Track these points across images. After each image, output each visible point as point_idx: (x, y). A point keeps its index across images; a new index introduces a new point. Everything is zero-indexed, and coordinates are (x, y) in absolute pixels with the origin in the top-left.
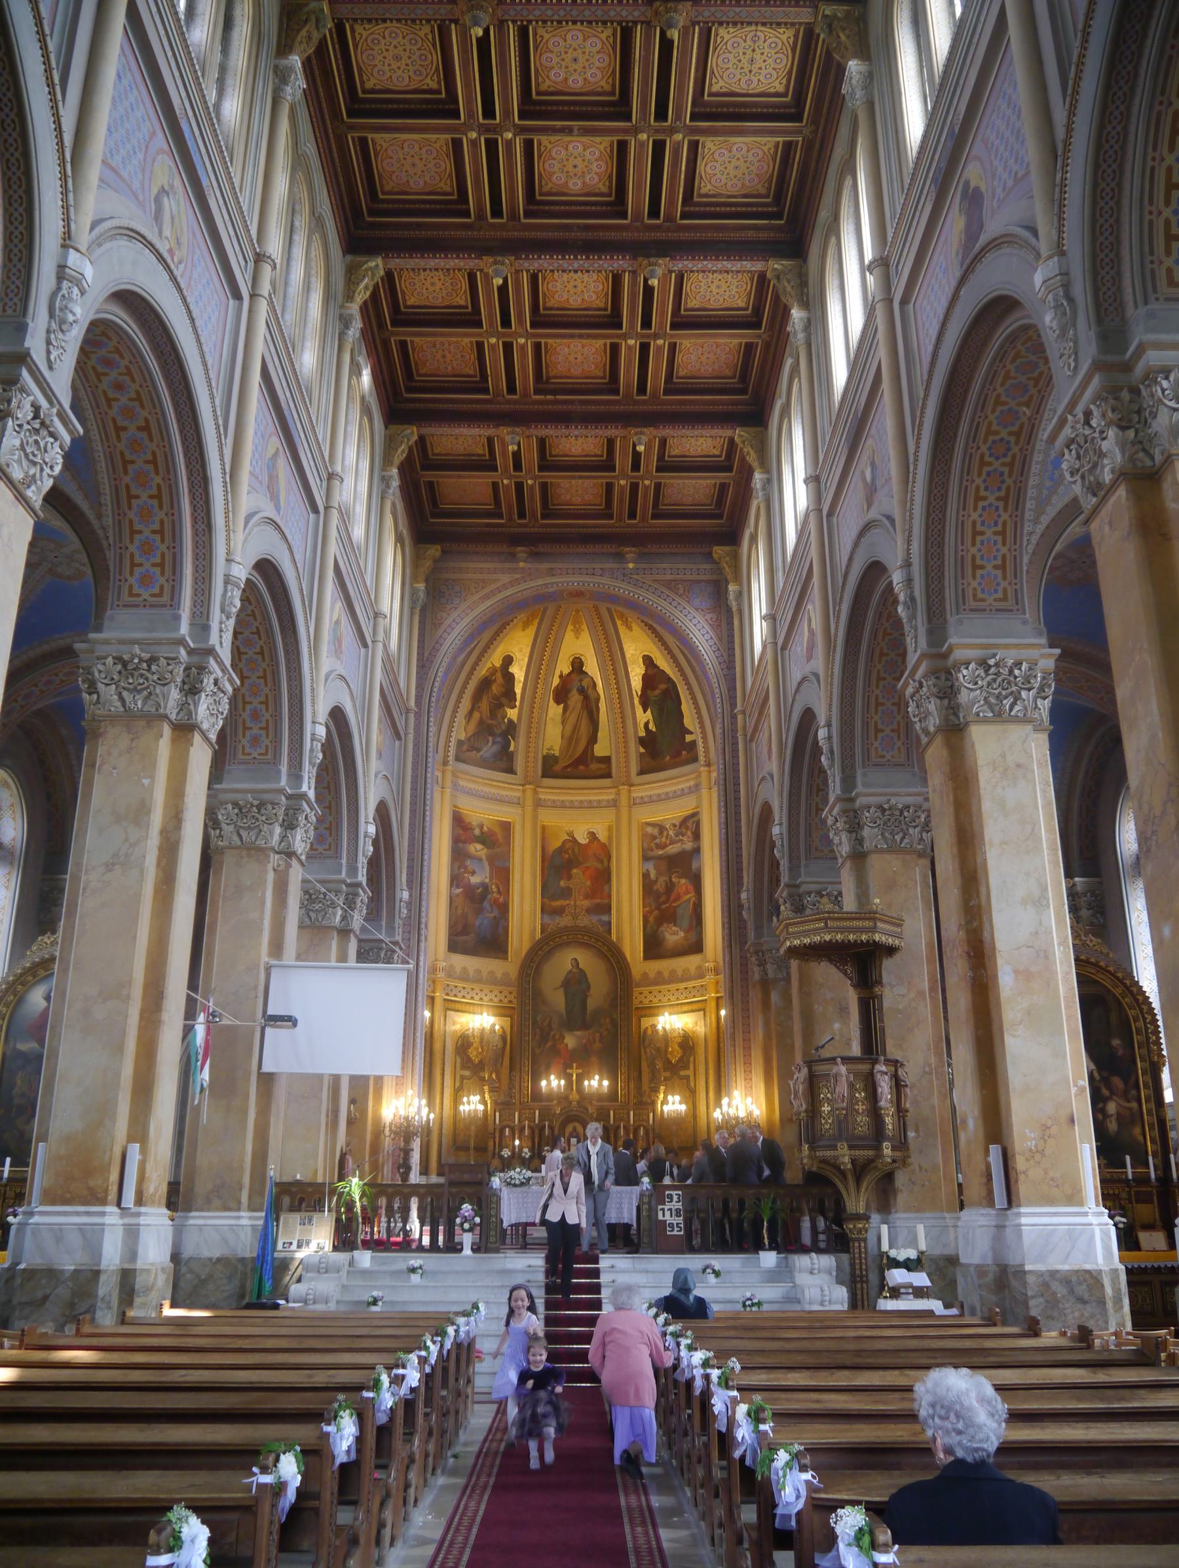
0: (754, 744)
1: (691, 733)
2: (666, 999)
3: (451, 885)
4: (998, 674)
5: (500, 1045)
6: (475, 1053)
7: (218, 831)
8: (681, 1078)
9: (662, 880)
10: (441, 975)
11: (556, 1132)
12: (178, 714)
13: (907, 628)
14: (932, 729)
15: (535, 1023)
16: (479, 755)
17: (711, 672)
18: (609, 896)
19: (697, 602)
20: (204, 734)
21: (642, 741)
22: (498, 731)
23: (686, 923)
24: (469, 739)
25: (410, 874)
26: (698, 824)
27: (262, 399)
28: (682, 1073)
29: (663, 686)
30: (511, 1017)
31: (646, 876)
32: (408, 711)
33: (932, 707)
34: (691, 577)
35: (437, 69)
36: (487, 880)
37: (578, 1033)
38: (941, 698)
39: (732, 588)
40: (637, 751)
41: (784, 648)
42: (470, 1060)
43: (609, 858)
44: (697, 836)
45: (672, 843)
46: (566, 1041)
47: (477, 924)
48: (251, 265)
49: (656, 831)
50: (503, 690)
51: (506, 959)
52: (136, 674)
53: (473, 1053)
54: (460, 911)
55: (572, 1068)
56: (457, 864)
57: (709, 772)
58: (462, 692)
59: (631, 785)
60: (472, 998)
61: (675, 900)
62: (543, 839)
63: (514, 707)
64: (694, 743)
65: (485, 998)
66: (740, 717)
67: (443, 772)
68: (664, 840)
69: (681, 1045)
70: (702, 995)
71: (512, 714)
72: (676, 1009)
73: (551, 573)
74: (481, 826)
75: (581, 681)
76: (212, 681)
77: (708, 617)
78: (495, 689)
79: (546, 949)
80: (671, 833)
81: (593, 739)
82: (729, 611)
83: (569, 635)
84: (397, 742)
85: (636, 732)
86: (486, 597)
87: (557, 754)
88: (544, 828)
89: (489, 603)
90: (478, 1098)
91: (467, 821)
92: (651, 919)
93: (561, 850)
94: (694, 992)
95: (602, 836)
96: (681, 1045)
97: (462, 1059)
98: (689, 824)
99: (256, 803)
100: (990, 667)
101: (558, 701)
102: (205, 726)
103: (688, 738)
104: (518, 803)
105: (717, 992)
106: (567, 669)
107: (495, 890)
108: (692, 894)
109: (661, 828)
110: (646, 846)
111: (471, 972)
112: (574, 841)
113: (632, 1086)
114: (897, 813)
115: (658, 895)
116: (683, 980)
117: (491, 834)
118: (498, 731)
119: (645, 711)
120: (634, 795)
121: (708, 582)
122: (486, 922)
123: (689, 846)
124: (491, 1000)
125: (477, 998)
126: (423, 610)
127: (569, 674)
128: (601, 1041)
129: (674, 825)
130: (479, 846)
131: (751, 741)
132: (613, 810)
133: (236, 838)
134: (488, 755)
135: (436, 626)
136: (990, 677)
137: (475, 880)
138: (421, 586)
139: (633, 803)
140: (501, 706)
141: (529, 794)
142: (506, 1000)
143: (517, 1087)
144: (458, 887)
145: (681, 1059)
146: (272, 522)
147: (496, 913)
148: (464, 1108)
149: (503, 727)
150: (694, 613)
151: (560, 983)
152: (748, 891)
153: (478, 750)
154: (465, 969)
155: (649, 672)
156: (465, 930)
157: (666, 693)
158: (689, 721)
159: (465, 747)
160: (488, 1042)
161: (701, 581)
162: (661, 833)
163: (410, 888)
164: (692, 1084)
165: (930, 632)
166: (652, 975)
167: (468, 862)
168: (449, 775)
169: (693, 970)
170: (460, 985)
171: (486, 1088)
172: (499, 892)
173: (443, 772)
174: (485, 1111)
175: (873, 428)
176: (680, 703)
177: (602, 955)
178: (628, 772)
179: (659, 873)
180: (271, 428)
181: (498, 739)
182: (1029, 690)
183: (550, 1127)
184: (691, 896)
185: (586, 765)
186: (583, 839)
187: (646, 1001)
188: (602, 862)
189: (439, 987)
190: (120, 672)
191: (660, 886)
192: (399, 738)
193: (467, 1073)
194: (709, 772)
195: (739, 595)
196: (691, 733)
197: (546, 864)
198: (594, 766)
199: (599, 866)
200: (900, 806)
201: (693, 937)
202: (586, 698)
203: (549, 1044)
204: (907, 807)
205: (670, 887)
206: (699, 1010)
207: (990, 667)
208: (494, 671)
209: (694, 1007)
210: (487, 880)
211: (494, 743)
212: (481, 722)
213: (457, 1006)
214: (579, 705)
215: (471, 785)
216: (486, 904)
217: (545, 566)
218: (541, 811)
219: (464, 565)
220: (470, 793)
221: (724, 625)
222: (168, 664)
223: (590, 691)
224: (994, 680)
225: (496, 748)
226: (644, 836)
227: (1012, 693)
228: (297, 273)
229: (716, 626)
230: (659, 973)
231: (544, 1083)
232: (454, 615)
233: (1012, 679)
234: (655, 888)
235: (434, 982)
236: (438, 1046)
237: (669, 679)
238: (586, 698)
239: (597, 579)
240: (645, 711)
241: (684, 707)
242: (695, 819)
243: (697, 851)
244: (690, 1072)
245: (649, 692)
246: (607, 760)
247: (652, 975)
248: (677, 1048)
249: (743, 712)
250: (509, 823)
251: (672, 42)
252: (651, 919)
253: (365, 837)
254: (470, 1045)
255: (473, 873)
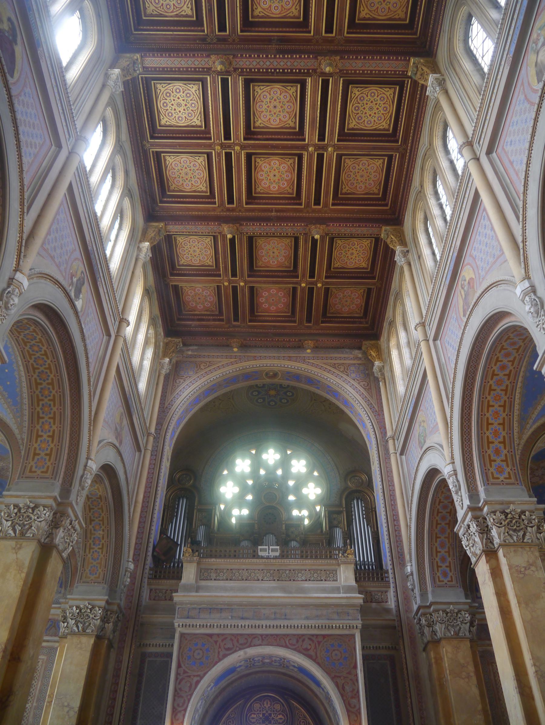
4: (513, 518)
7: (66, 624)
12: (45, 540)
13: (455, 497)
14: (478, 552)
20: (60, 553)
27: (115, 384)
33: (477, 539)
35: (212, 257)
38: (482, 533)
48: (117, 323)
52: (25, 515)
76: (68, 521)
99: (90, 607)
100: (508, 514)
102: (61, 547)
114: (455, 615)
133: (75, 629)
136: (508, 520)
146: (115, 446)
165: (471, 498)
175: (424, 405)
180: (120, 404)
182: (532, 527)
190: (16, 514)
200: (456, 611)
204: (523, 512)
207: (508, 514)
222: (44, 510)
224: (511, 522)
227: (522, 529)
228: (141, 337)
233: (521, 520)
251: (317, 240)
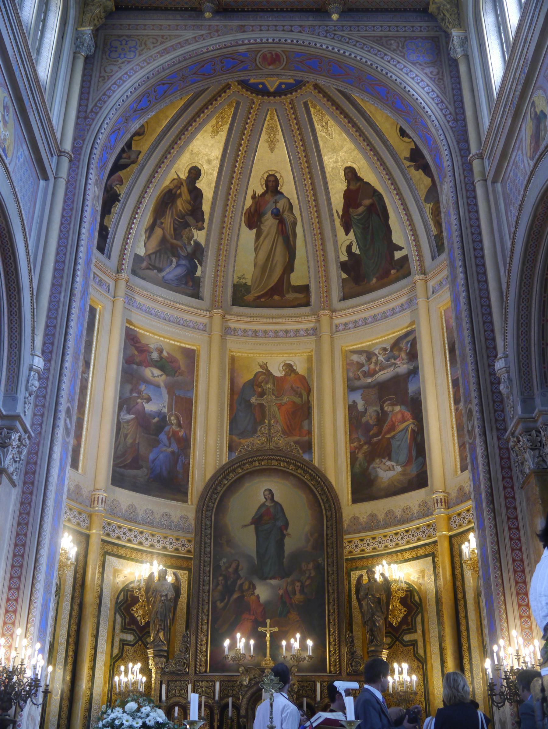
0: (499, 186)
1: (401, 248)
2: (382, 547)
3: (120, 408)
5: (171, 595)
6: (141, 612)
8: (406, 644)
9: (372, 411)
10: (99, 507)
11: (243, 712)
15: (217, 567)
16: (161, 275)
17: (436, 133)
18: (310, 433)
19: (413, 57)
21: (344, 266)
22: (183, 253)
23: (403, 457)
24: (149, 256)
25: (49, 335)
26: (414, 343)
28: (407, 638)
29: (367, 202)
30: (189, 570)
31: (352, 408)
32: (61, 153)
34: (406, 34)
36: (165, 410)
37: (273, 582)
39: (455, 33)
40: (339, 277)
41: (494, 182)
42: (134, 620)
43: (309, 391)
44: (413, 356)
45: (382, 368)
46: (257, 592)
47: (151, 456)
49: (362, 359)
50: (190, 208)
51: (186, 501)
53: (138, 612)
54: (129, 441)
55: (265, 625)
56: (128, 387)
57: (426, 281)
58: (142, 197)
59: (334, 311)
60: (140, 543)
61: (388, 432)
62: (232, 371)
63: (202, 228)
64: (405, 258)
65: (158, 546)
66: (476, 164)
67: (116, 281)
68: (372, 366)
69: (404, 601)
70: (430, 537)
71: (200, 236)
72: (395, 557)
73: (242, 29)
74: (160, 351)
75: (276, 202)
77: (428, 70)
78: (181, 205)
79: (233, 477)
80: (381, 358)
81: (289, 267)
82: (454, 63)
83: (262, 146)
84: (42, 183)
85: (337, 257)
86: (166, 51)
87: (249, 283)
88: (233, 360)
89: (168, 57)
90: (139, 665)
91: (144, 342)
92: (360, 456)
93: (253, 383)
94: (419, 534)
95: (301, 368)
96: (404, 601)
97: (123, 616)
98: (403, 345)
101: (250, 226)
103: (398, 255)
104: (206, 329)
105: (450, 530)
106: (260, 191)
107: (174, 421)
108: (411, 421)
109: (369, 355)
110: (351, 375)
111: (141, 513)
112: (268, 373)
113: (344, 650)
115: (367, 428)
116: (402, 522)
117: (172, 360)
118: (183, 253)
119: (347, 234)
120: (336, 321)
121: (426, 38)
122: (161, 456)
123: (403, 368)
124: (165, 548)
125: (147, 544)
126: (88, 60)
127: (263, 195)
128: (302, 591)
129: (385, 349)
130: (157, 372)
131: (494, 182)
132: (313, 338)
134: (171, 276)
135: (104, 79)
137: (150, 408)
138: (87, 30)
139: (335, 329)
140: (187, 225)
141: (217, 320)
142: (183, 550)
143: (192, 650)
144: (129, 412)
145: (404, 620)
147: (174, 447)
148: (121, 679)
149: (189, 249)
150: (410, 66)
151: (249, 520)
152: (506, 357)
153: (160, 270)
154: (132, 507)
155: (352, 187)
156: (135, 464)
157: (371, 209)
158: (397, 238)
159: (144, 264)
160: (155, 591)
161: (417, 37)
162: (369, 359)
163: (47, 354)
164: (421, 652)
166: (363, 519)
167: (143, 387)
168: (122, 284)
169: (415, 509)
170: (126, 525)
171: (150, 652)
172: (179, 425)
173: (116, 281)
174: (148, 685)
176: (386, 217)
177: (302, 485)
178: (329, 296)
179: (367, 403)
181: (183, 262)
183: (236, 707)
184: (410, 424)
185: (282, 295)
186: (277, 371)
187: (357, 551)
188: (301, 396)
189: (96, 522)
191: (370, 417)
192: (46, 178)
193: (130, 637)
194: (426, 281)
195: (465, 40)
196: (401, 248)
197: (236, 397)
198: (290, 296)
199: (297, 400)
201: (413, 470)
202: (282, 222)
203: (235, 596)
205: (382, 417)
206: (426, 556)
208: (178, 183)
209: (419, 552)
210: (165, 410)
211: (178, 265)
212: (164, 240)
213: (120, 551)
214: (274, 230)
215: (149, 304)
216: (163, 437)
217: (235, 23)
218: (229, 338)
219: (140, 22)
220: (148, 311)
221: (447, 79)
223: (286, 215)
225: (180, 271)
226: (349, 365)
229: (438, 79)
230: (372, 516)
231: (227, 643)
232: (126, 68)
234: (364, 420)
235: (90, 516)
236: (90, 598)
237: (375, 193)
238: (282, 222)
239: (295, 36)
240: (347, 234)
241: (391, 222)
242: (411, 338)
243: (414, 372)
244: (417, 636)
245: (351, 210)
246: (305, 289)
247: (363, 519)
248: (399, 606)
249: (481, 156)
250: (193, 351)
252: (360, 456)
253: (31, 369)
254: (135, 600)
255: (149, 400)
